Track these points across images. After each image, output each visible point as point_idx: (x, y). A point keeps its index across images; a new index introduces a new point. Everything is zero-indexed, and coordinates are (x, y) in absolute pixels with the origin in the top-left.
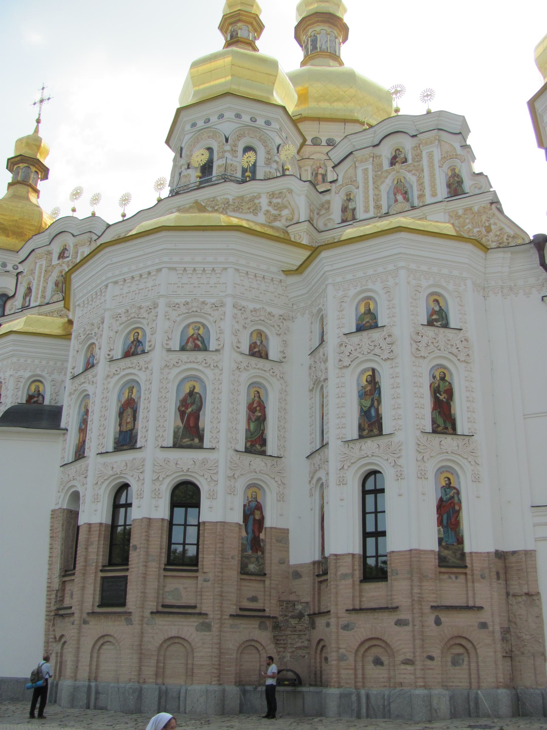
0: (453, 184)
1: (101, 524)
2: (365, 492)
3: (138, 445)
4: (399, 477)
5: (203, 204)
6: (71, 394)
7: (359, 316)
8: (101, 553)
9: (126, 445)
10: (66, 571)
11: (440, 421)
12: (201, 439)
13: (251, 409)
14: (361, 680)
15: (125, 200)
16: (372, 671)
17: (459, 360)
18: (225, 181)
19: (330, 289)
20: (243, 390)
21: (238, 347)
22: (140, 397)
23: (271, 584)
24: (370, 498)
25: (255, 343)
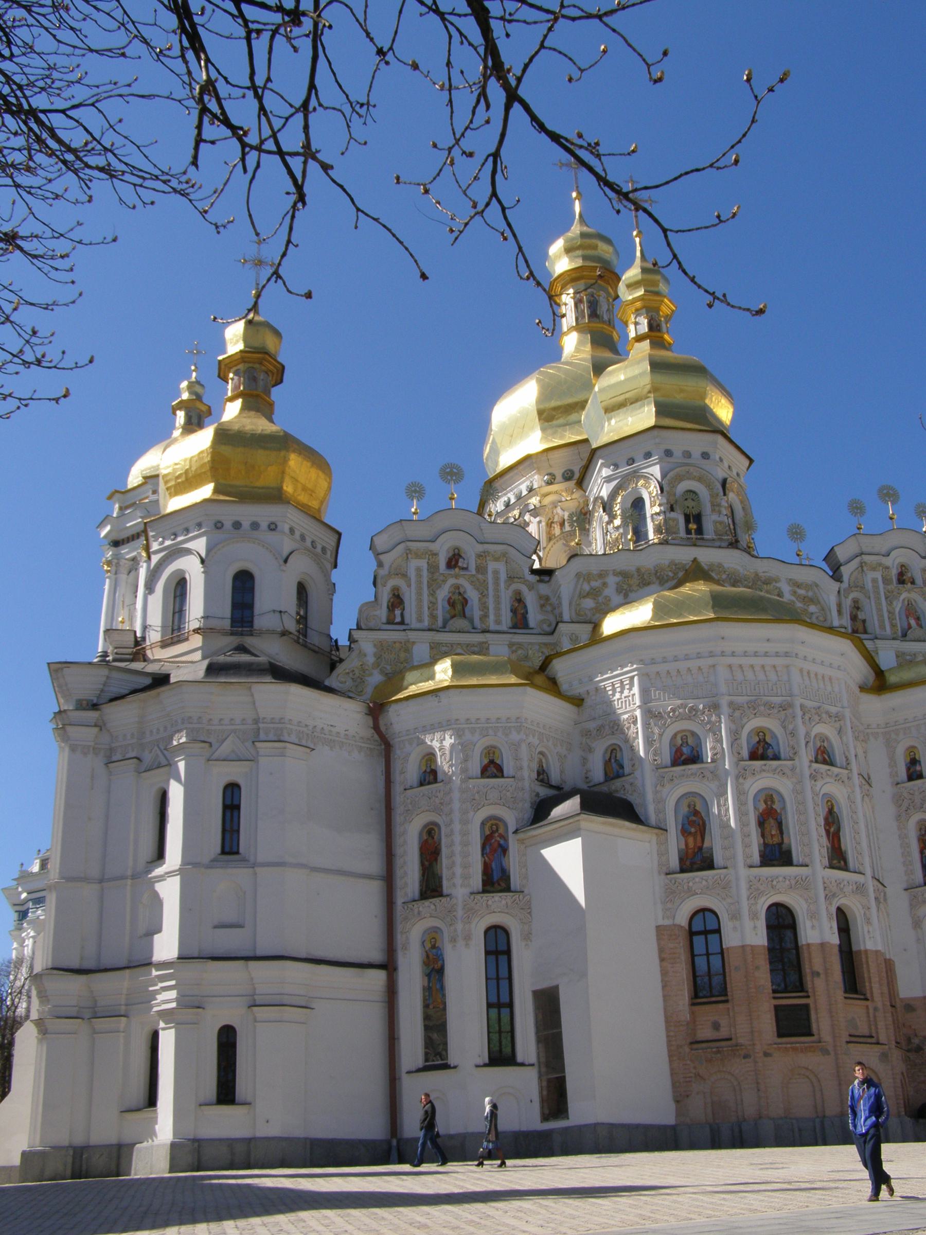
5: (706, 567)
22: (784, 808)
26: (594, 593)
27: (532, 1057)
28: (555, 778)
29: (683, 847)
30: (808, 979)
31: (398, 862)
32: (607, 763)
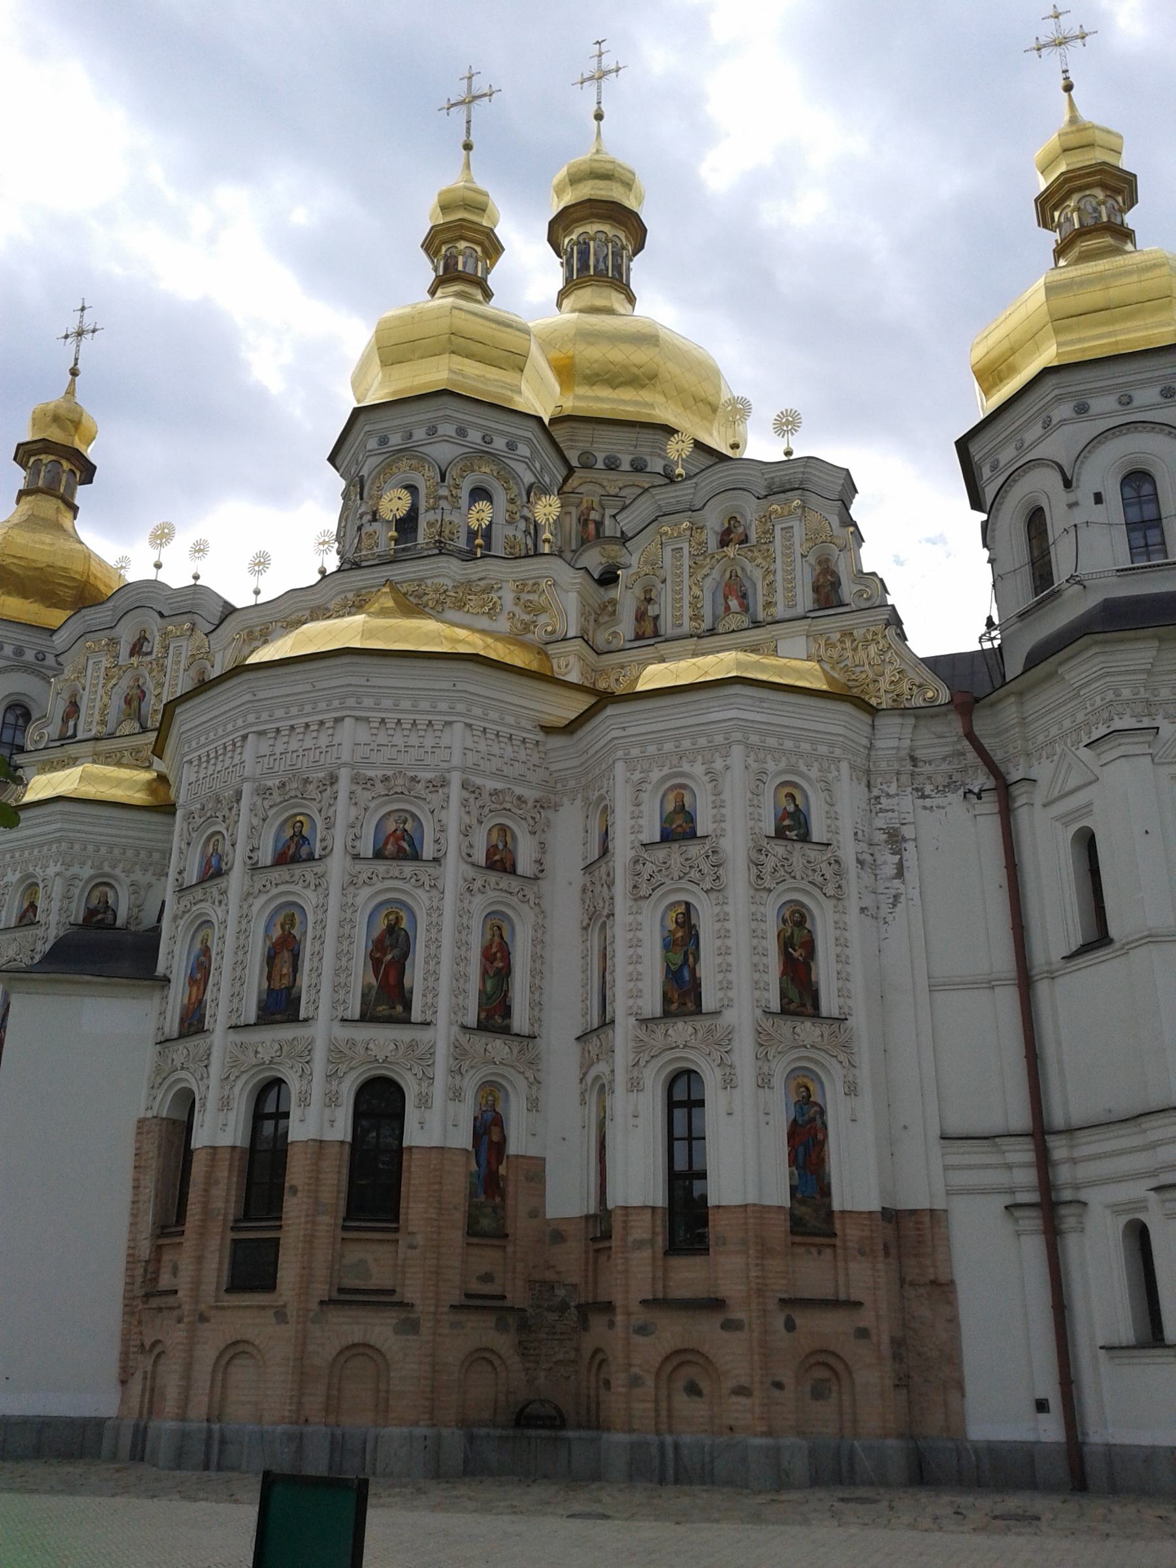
0: (824, 587)
1: (233, 1148)
2: (672, 1105)
3: (302, 1015)
4: (729, 1083)
6: (175, 918)
7: (664, 816)
8: (233, 1199)
9: (280, 1013)
10: (163, 1227)
11: (793, 993)
12: (408, 1006)
13: (488, 956)
14: (665, 1420)
15: (261, 563)
16: (684, 1404)
17: (825, 894)
18: (441, 554)
19: (620, 765)
20: (476, 924)
21: (469, 855)
23: (515, 1252)
24: (680, 1114)
25: (496, 846)
29: (186, 1001)
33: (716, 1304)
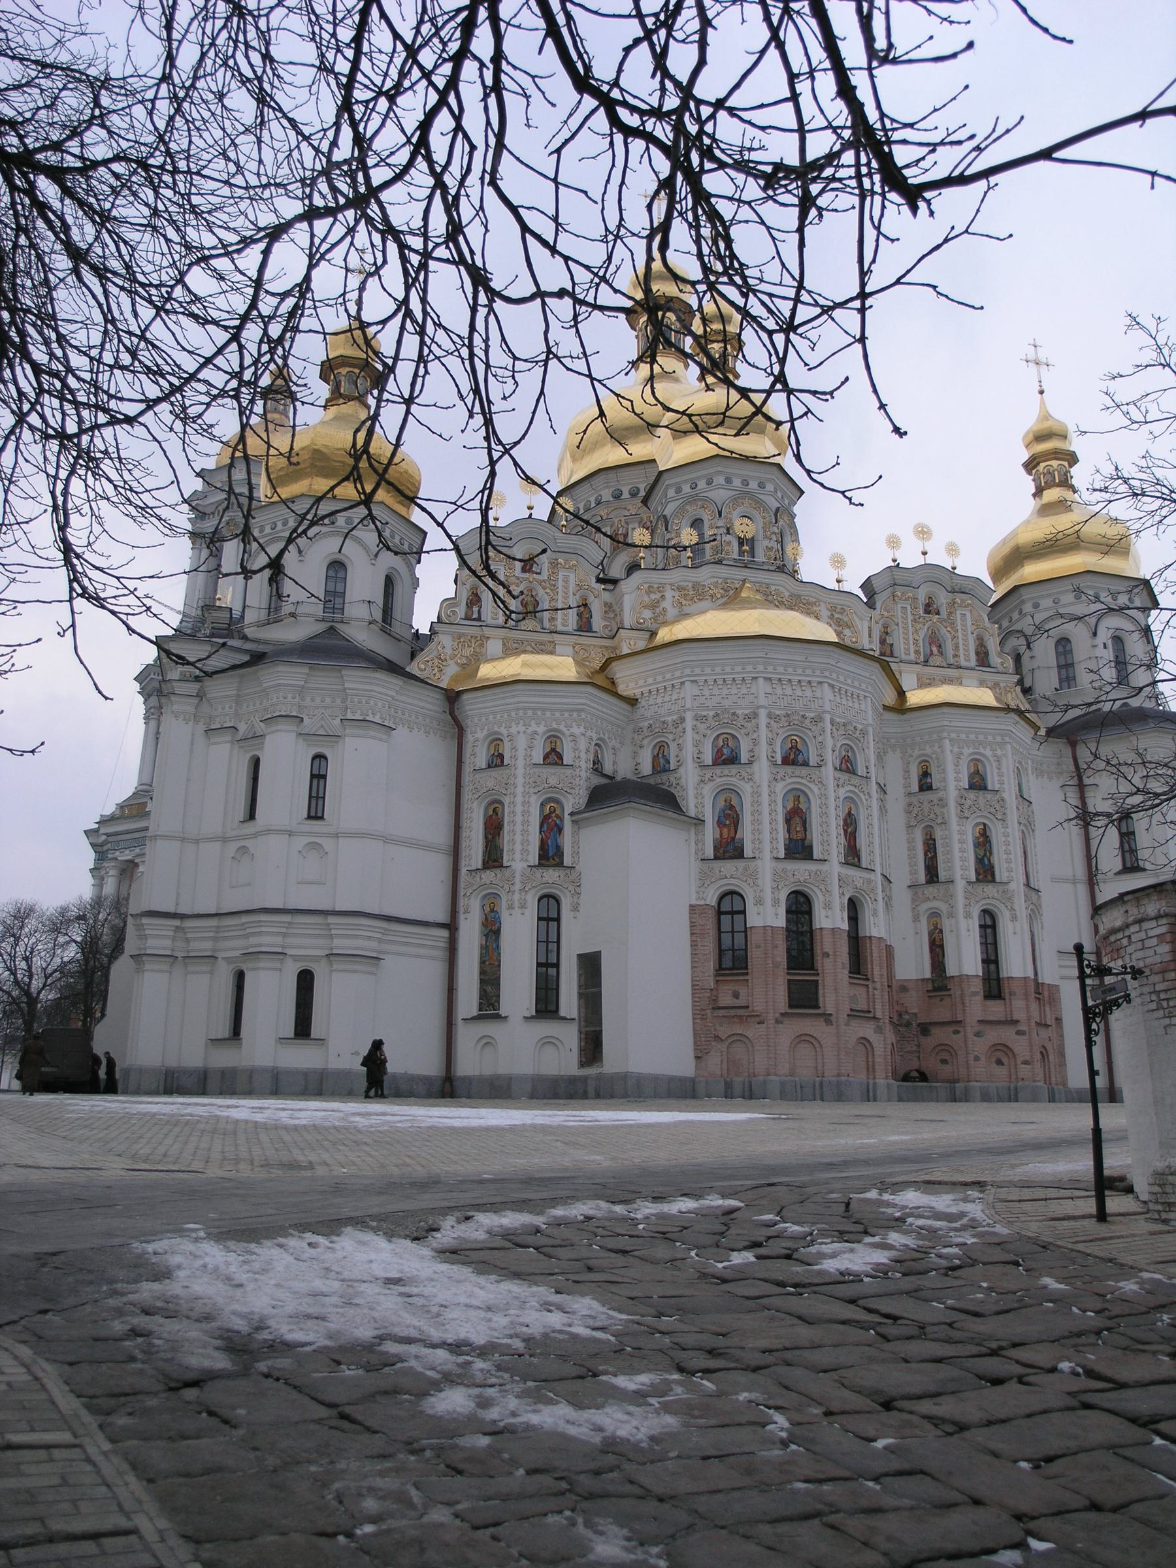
4: (1014, 918)
19: (947, 742)
22: (809, 808)
26: (653, 606)
27: (575, 1015)
28: (608, 769)
30: (818, 958)
31: (464, 834)
32: (655, 758)
33: (1015, 1022)
